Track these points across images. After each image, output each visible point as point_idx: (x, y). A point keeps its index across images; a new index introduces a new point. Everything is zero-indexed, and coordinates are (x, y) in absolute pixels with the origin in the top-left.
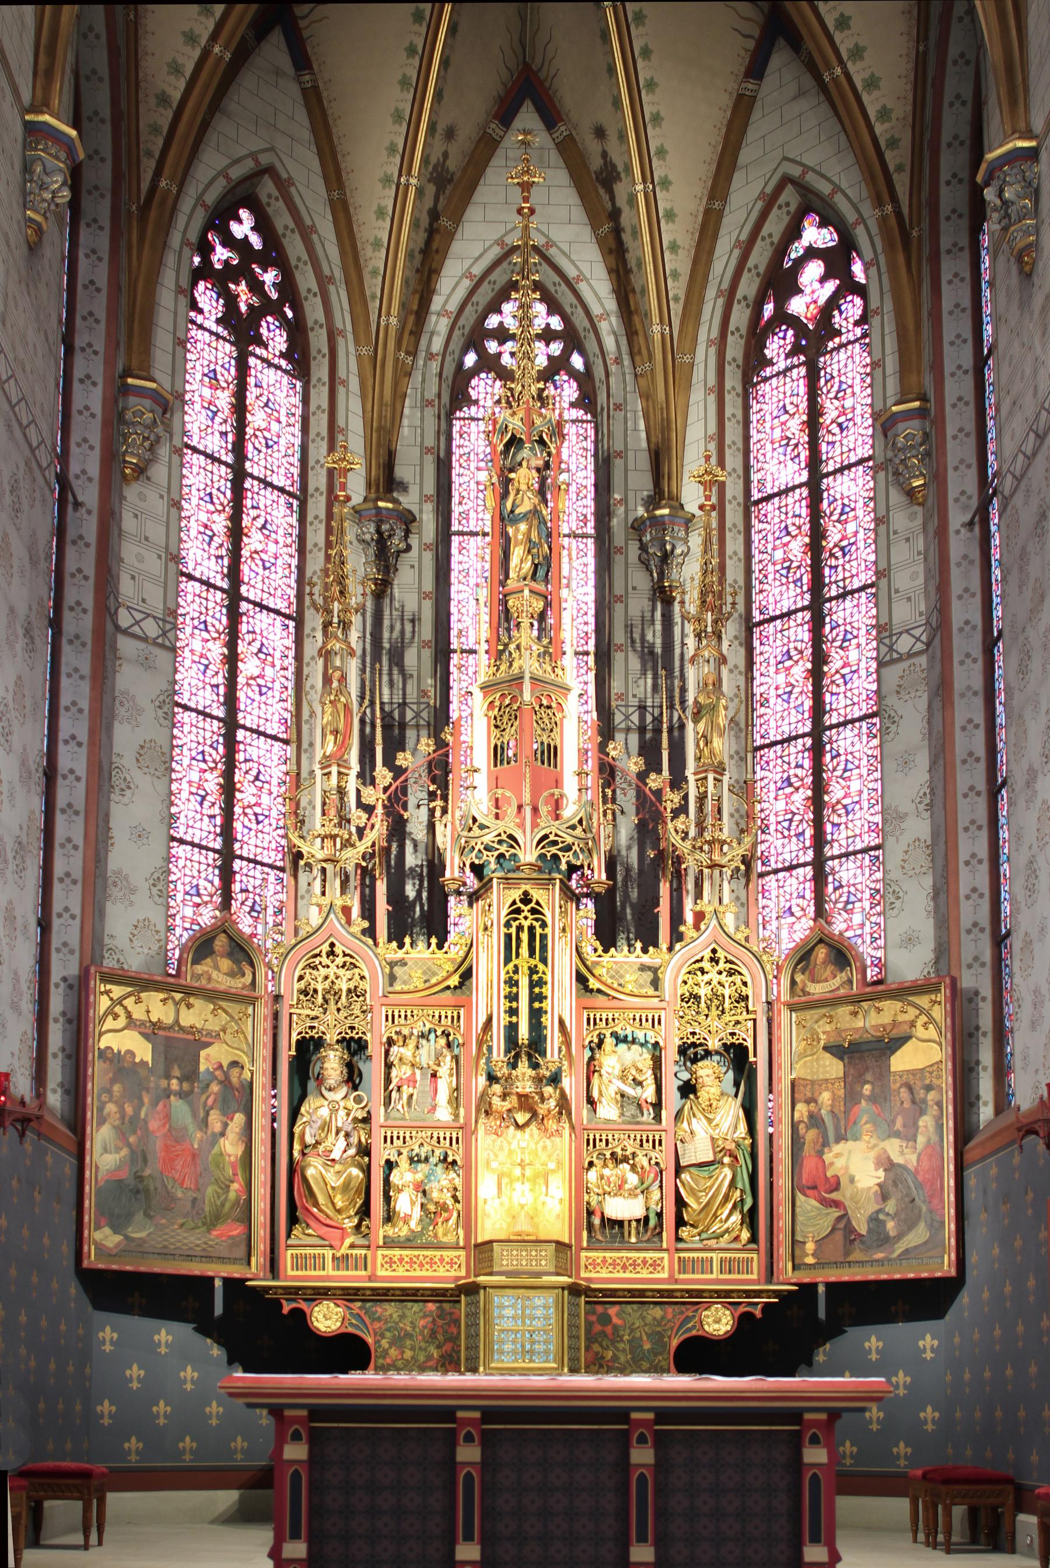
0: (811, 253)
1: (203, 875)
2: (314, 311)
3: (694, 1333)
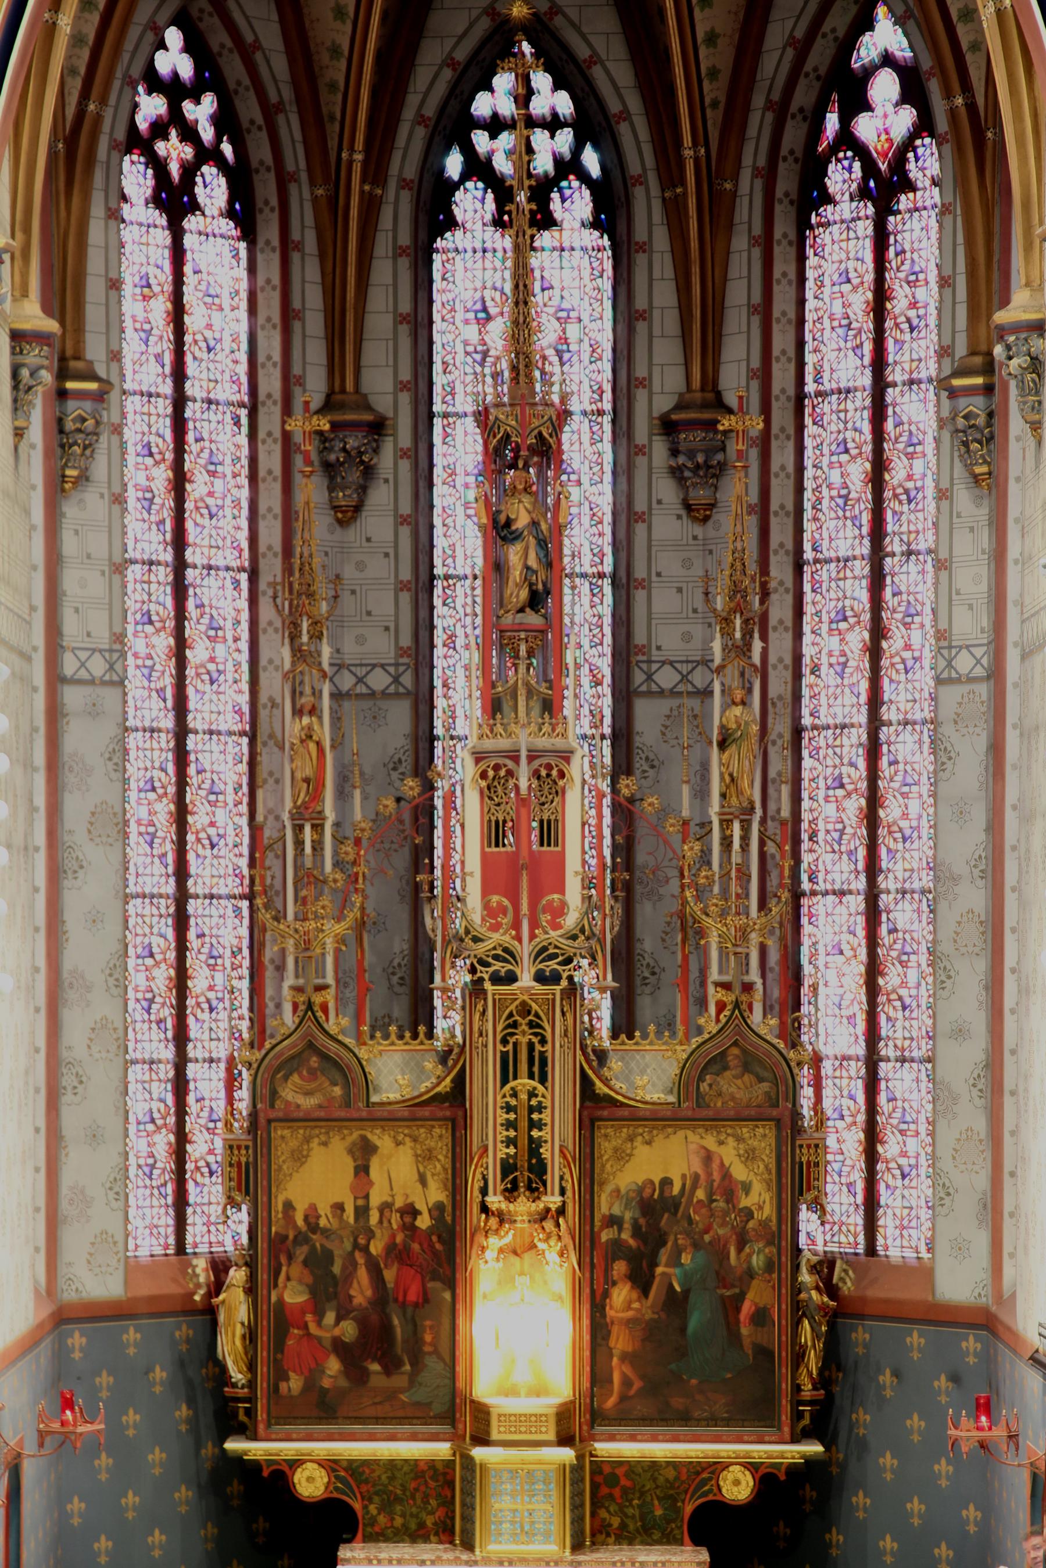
0: (887, 60)
1: (155, 930)
2: (260, 151)
3: (711, 1497)
